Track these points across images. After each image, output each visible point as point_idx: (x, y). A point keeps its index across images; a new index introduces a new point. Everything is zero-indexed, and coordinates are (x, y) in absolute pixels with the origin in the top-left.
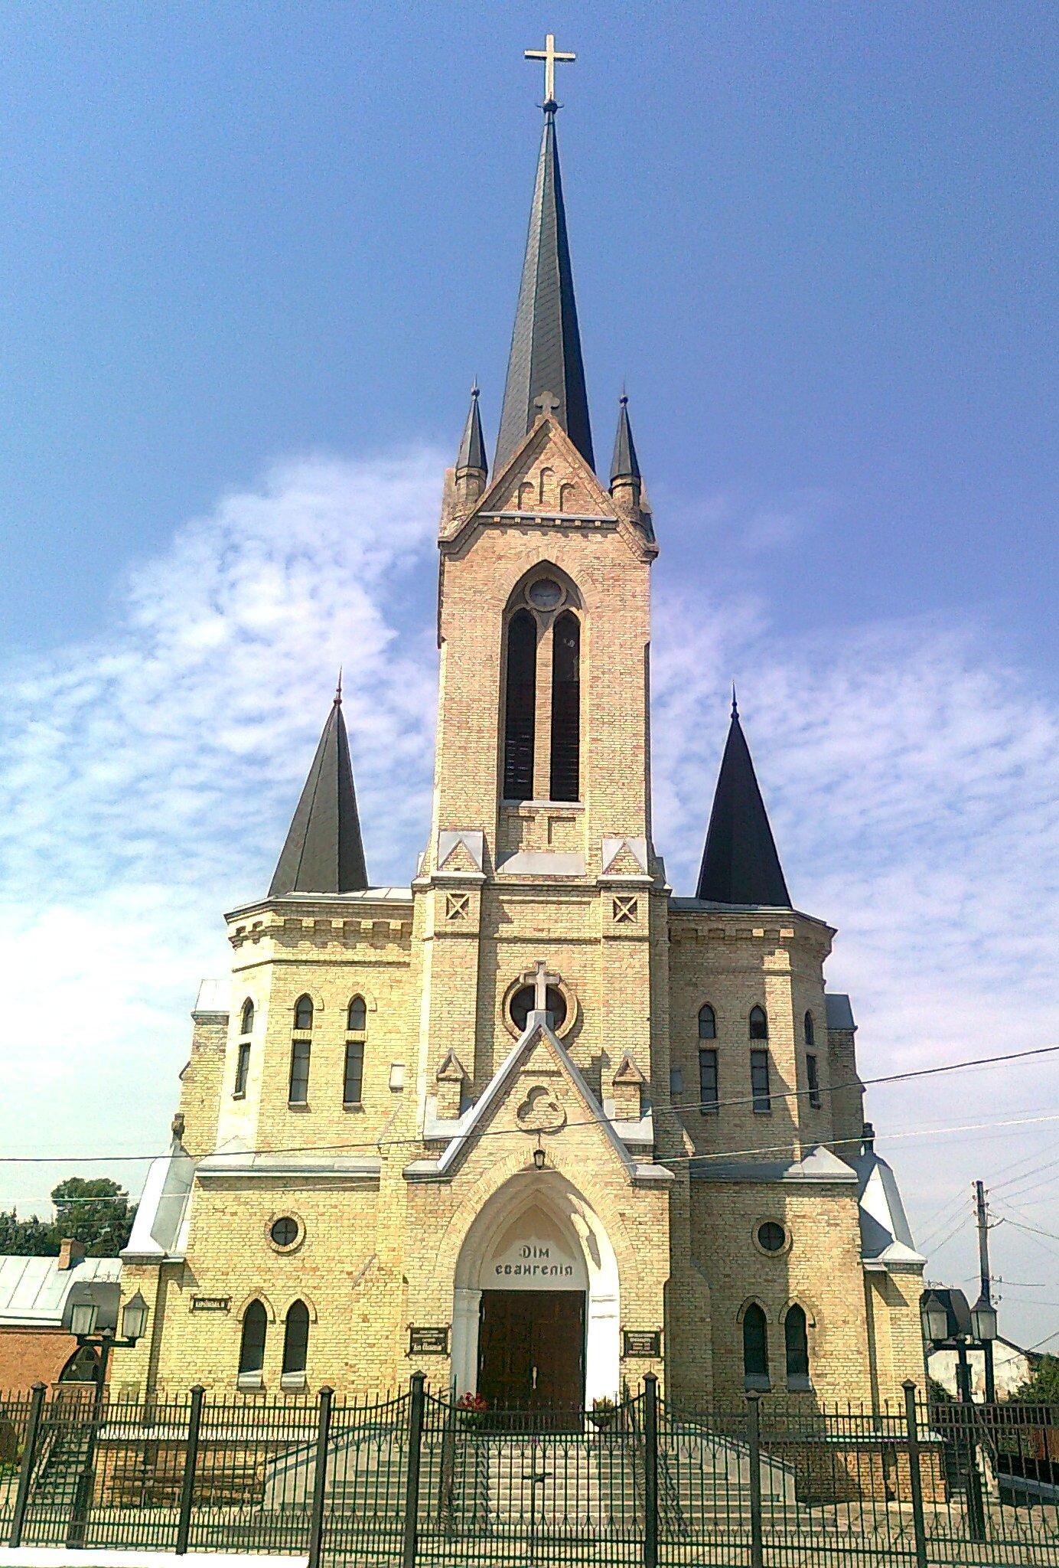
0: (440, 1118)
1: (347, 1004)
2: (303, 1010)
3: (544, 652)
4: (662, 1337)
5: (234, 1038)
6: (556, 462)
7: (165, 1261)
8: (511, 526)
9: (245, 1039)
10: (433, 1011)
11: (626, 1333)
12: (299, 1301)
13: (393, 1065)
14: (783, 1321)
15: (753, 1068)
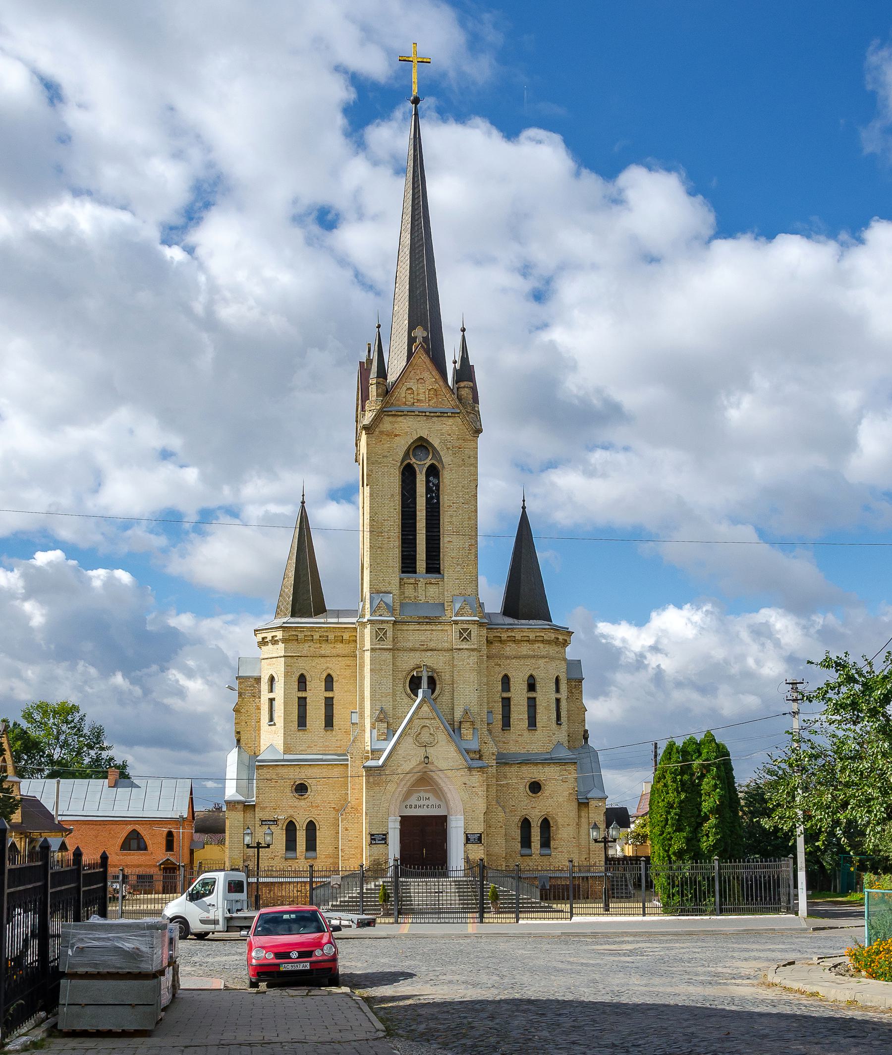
0: (378, 740)
2: (302, 681)
4: (483, 836)
5: (265, 696)
6: (426, 375)
8: (401, 416)
9: (271, 696)
11: (467, 834)
12: (311, 821)
14: (539, 825)
15: (528, 706)
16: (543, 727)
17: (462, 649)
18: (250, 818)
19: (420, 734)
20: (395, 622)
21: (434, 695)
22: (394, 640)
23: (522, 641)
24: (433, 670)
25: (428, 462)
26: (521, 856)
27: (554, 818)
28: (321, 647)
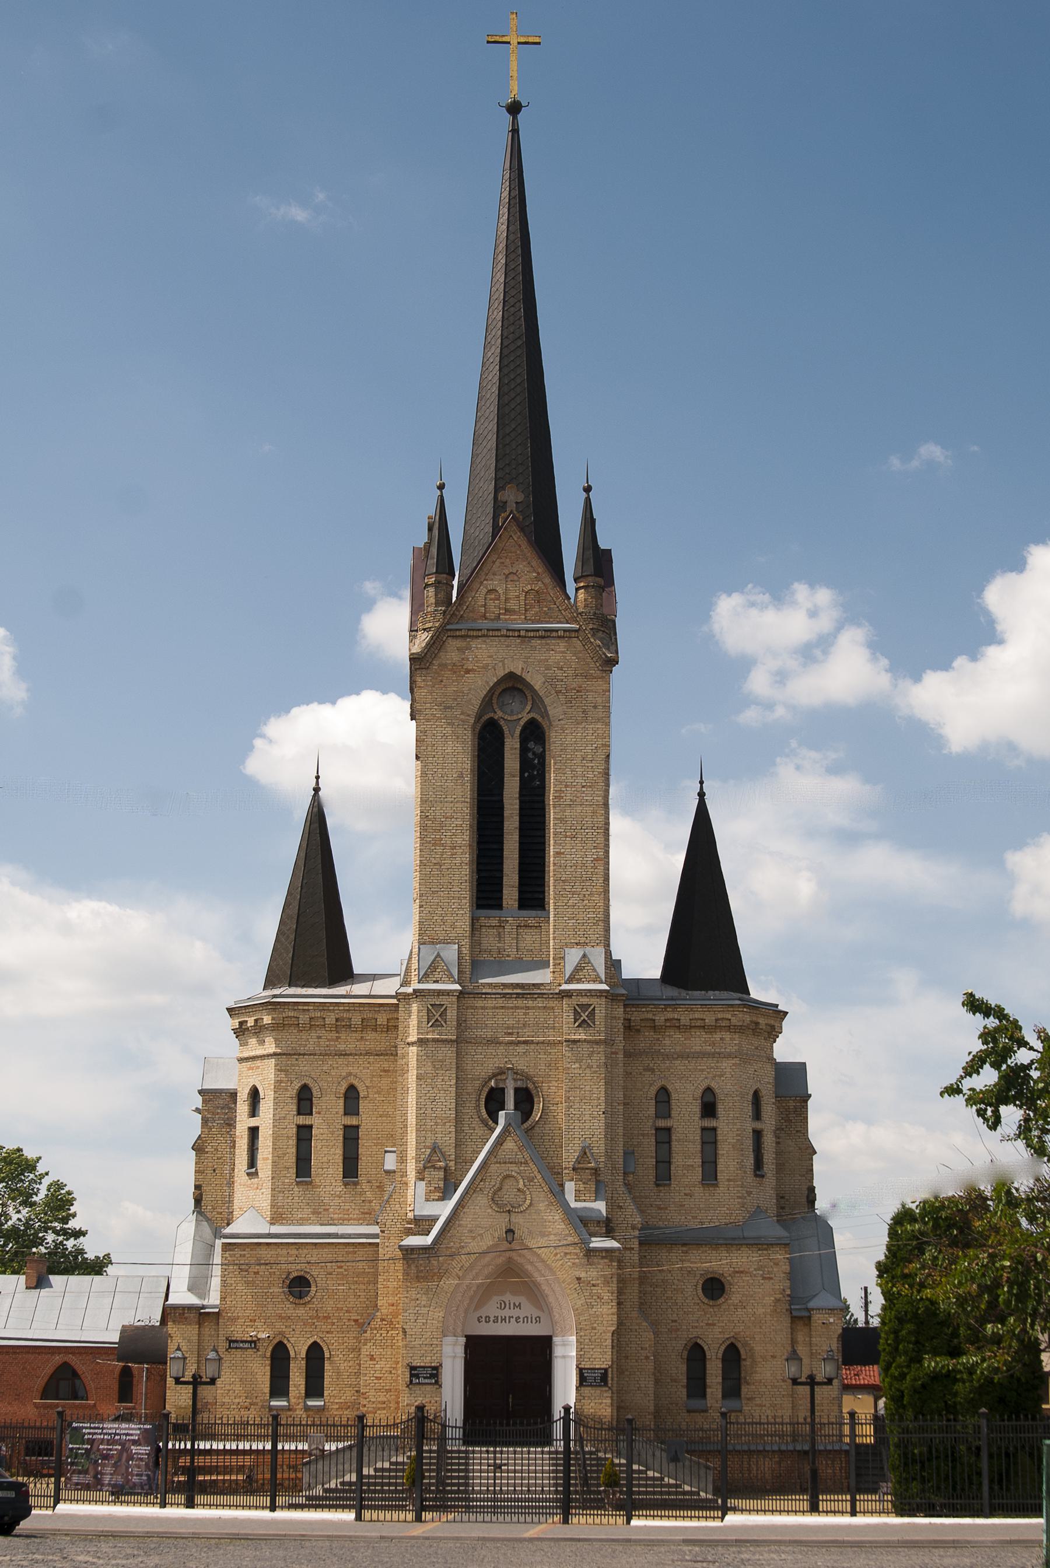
0: (427, 1200)
1: (343, 1091)
3: (512, 763)
5: (243, 1122)
6: (521, 567)
7: (202, 1311)
8: (477, 637)
9: (253, 1122)
10: (418, 1109)
12: (315, 1343)
13: (386, 1152)
15: (703, 1143)
16: (729, 1180)
17: (579, 1041)
18: (210, 1335)
19: (500, 1189)
20: (461, 992)
21: (529, 1122)
22: (459, 1025)
23: (691, 1027)
24: (528, 1078)
25: (525, 717)
26: (688, 1411)
27: (746, 1344)
28: (338, 1038)
